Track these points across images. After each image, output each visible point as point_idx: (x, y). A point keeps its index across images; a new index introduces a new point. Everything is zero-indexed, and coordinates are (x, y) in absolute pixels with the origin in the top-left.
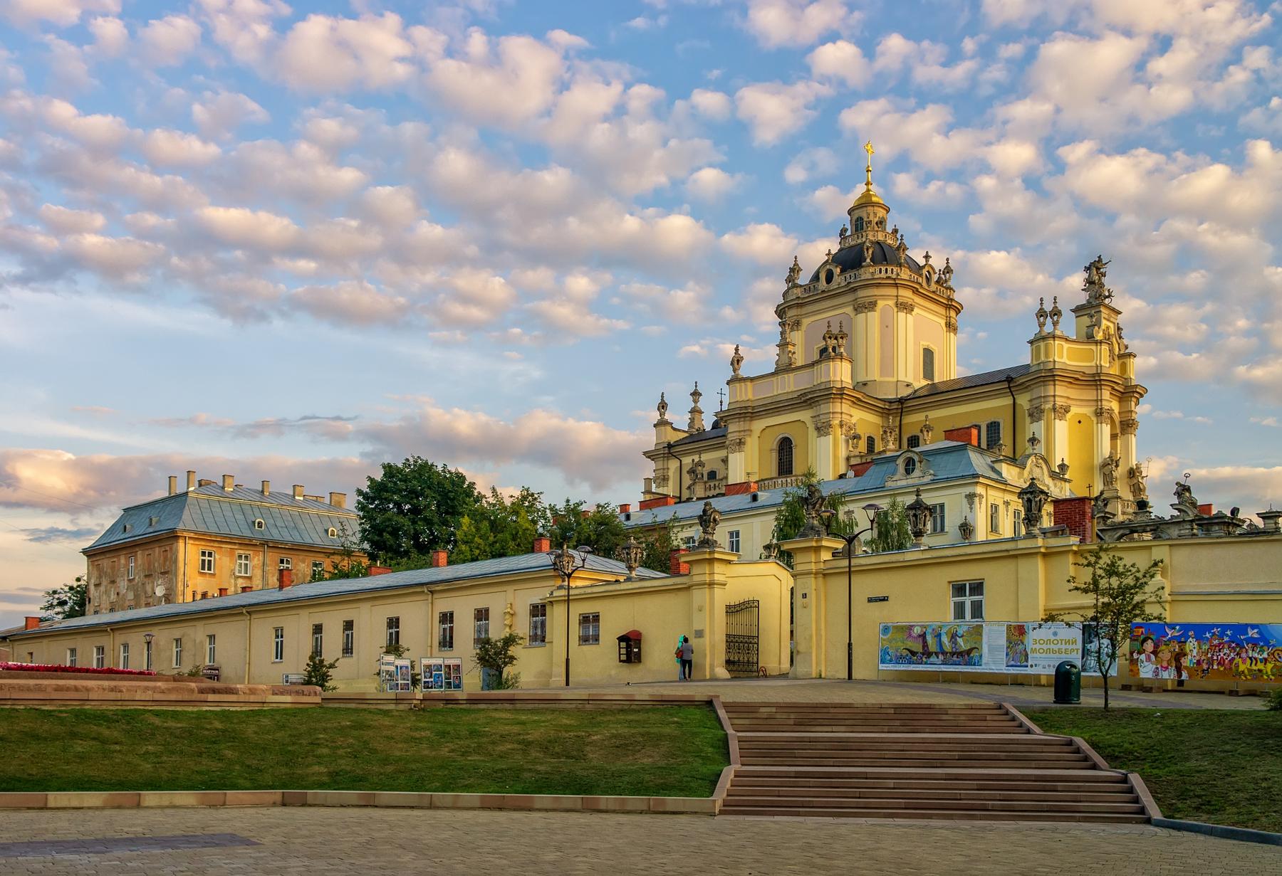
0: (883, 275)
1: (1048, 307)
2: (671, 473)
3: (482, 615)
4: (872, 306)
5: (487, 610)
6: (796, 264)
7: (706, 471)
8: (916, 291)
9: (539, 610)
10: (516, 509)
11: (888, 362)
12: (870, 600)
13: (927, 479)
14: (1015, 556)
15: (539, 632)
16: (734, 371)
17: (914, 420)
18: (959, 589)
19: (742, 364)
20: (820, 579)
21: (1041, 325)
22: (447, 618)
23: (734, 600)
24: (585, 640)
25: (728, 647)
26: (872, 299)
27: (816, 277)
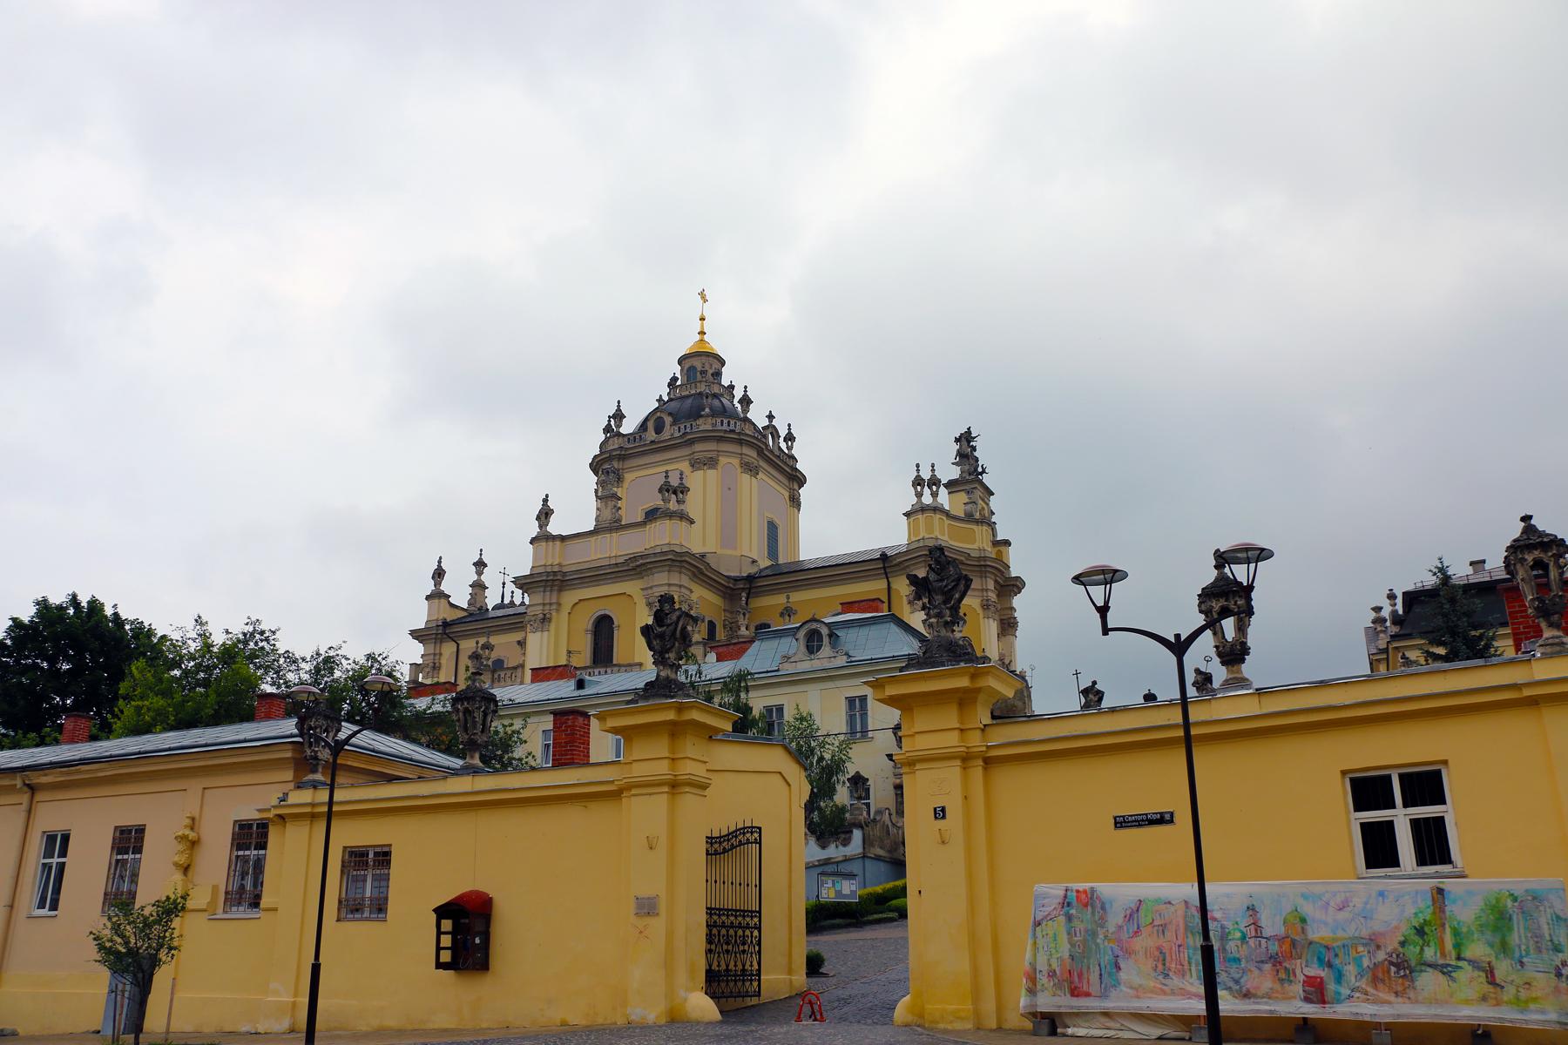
0: (725, 427)
1: (926, 475)
2: (444, 661)
3: (129, 840)
4: (711, 463)
5: (141, 830)
6: (619, 409)
7: (494, 655)
8: (760, 453)
9: (251, 836)
10: (229, 654)
11: (729, 531)
12: (1121, 823)
13: (841, 661)
14: (1534, 702)
15: (249, 887)
16: (540, 527)
17: (772, 602)
18: (1369, 791)
19: (552, 518)
20: (977, 772)
21: (919, 495)
22: (58, 843)
23: (722, 826)
24: (351, 908)
25: (710, 941)
26: (713, 455)
27: (643, 426)
